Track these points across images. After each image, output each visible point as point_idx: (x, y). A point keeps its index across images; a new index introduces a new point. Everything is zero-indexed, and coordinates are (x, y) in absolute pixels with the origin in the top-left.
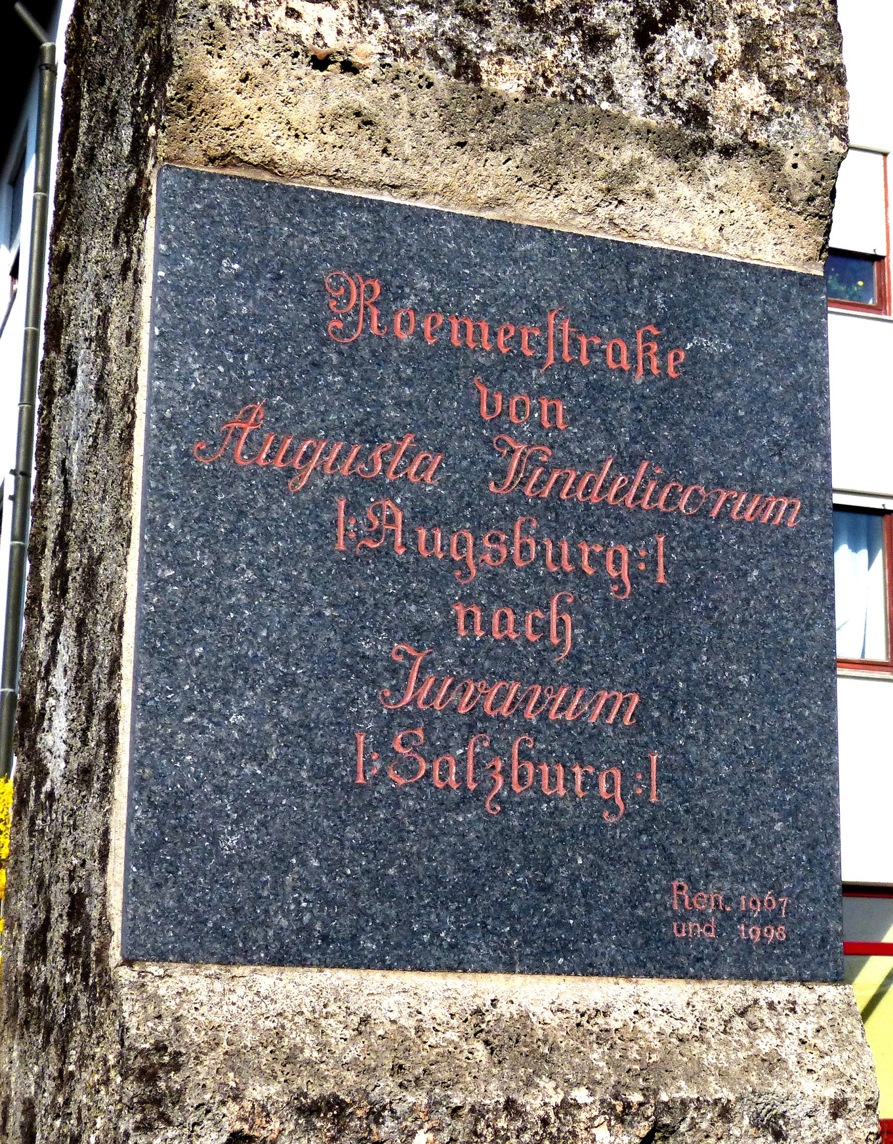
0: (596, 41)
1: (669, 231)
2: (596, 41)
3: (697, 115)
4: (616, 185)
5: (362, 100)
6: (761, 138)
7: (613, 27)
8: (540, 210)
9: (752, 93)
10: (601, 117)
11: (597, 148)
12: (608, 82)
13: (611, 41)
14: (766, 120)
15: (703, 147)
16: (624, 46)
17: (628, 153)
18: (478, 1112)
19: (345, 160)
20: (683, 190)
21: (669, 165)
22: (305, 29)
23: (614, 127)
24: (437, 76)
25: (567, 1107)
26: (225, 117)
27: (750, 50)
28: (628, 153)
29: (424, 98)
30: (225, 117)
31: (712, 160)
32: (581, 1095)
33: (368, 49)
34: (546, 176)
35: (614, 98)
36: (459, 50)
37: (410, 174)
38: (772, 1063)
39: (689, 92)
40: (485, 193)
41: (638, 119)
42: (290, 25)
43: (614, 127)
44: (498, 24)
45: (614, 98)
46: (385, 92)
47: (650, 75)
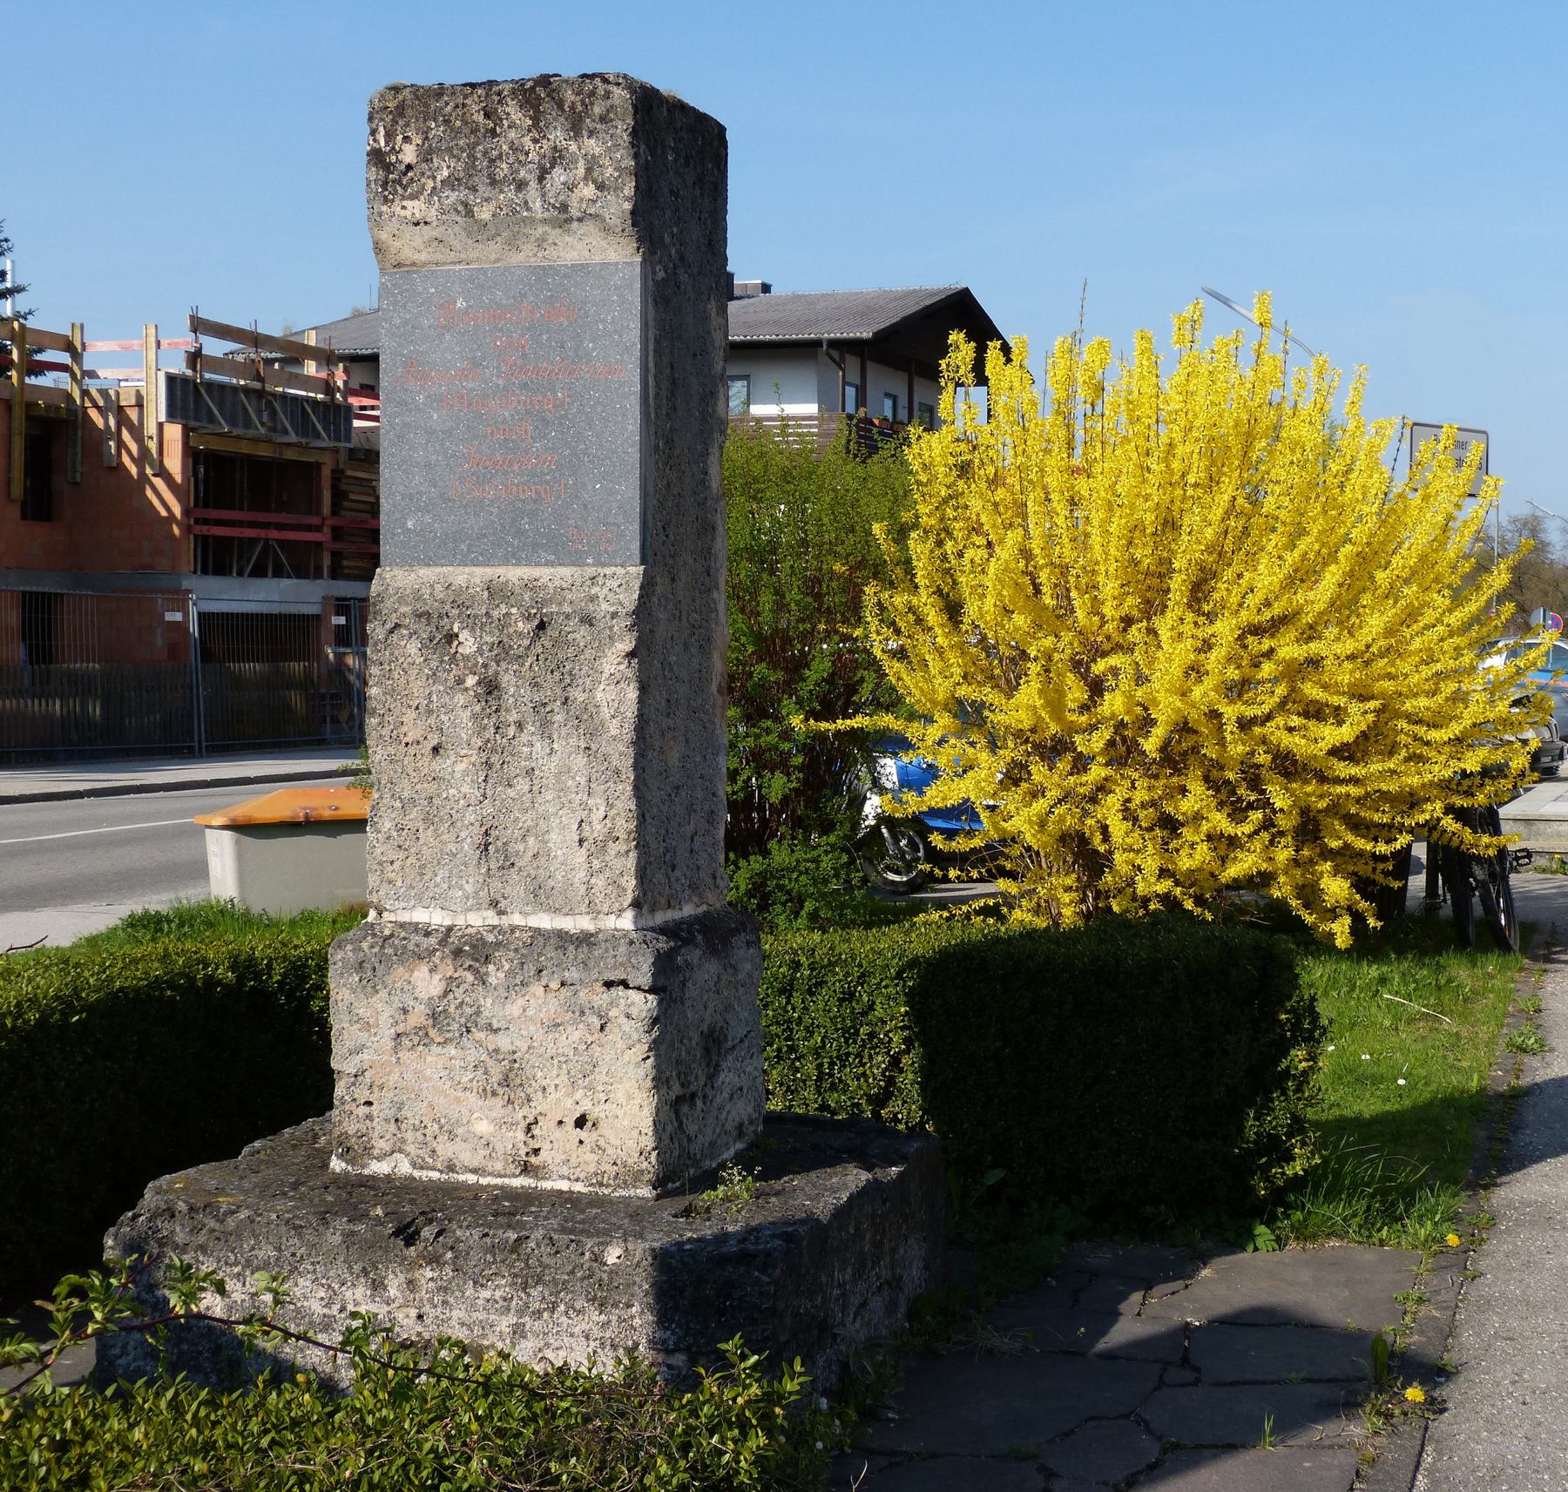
0: (521, 185)
1: (568, 256)
2: (521, 185)
3: (564, 207)
4: (541, 242)
5: (435, 234)
6: (592, 211)
7: (528, 177)
8: (516, 259)
9: (589, 191)
10: (524, 220)
11: (528, 230)
12: (526, 202)
13: (527, 184)
14: (594, 202)
15: (569, 220)
16: (533, 184)
17: (540, 230)
18: (476, 616)
19: (439, 257)
20: (568, 239)
21: (558, 231)
22: (408, 213)
23: (531, 221)
24: (459, 219)
25: (508, 614)
26: (393, 251)
27: (589, 170)
28: (540, 230)
29: (457, 228)
30: (393, 251)
31: (575, 225)
32: (514, 610)
33: (432, 214)
34: (513, 244)
35: (529, 209)
36: (466, 205)
37: (463, 256)
38: (593, 599)
39: (561, 198)
40: (493, 257)
41: (540, 216)
42: (403, 213)
43: (531, 221)
44: (481, 188)
45: (529, 209)
46: (442, 229)
47: (543, 195)
